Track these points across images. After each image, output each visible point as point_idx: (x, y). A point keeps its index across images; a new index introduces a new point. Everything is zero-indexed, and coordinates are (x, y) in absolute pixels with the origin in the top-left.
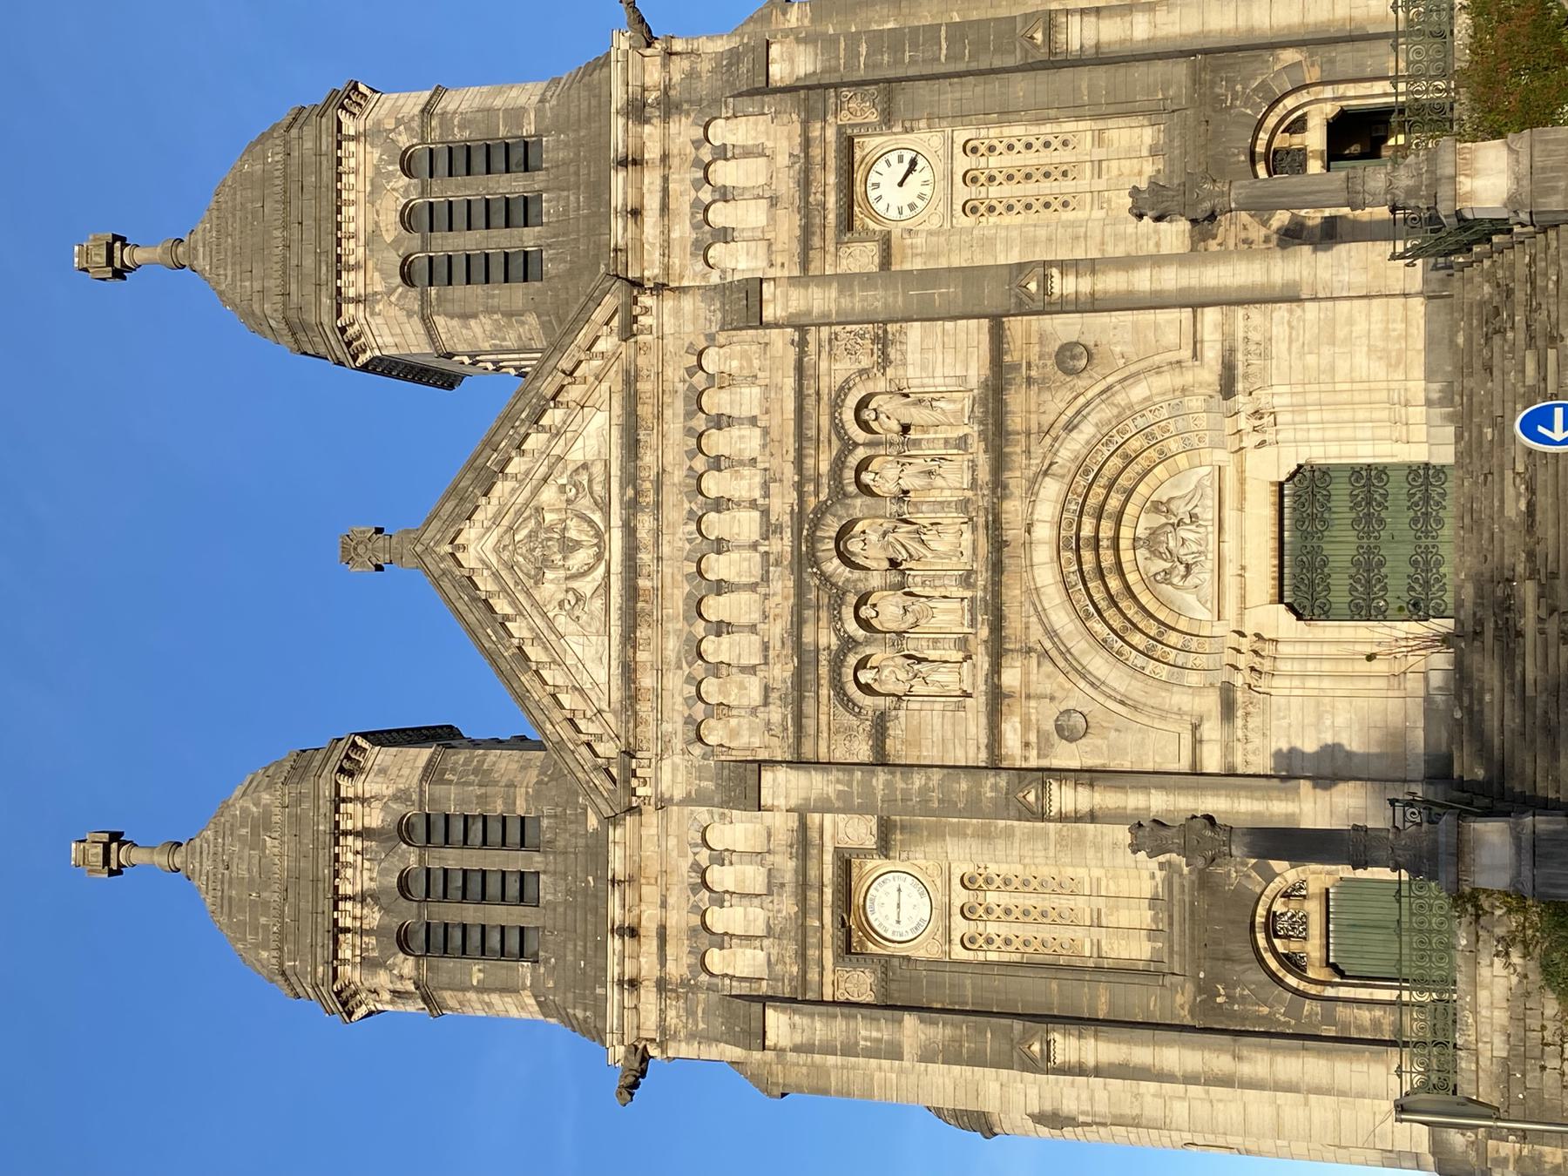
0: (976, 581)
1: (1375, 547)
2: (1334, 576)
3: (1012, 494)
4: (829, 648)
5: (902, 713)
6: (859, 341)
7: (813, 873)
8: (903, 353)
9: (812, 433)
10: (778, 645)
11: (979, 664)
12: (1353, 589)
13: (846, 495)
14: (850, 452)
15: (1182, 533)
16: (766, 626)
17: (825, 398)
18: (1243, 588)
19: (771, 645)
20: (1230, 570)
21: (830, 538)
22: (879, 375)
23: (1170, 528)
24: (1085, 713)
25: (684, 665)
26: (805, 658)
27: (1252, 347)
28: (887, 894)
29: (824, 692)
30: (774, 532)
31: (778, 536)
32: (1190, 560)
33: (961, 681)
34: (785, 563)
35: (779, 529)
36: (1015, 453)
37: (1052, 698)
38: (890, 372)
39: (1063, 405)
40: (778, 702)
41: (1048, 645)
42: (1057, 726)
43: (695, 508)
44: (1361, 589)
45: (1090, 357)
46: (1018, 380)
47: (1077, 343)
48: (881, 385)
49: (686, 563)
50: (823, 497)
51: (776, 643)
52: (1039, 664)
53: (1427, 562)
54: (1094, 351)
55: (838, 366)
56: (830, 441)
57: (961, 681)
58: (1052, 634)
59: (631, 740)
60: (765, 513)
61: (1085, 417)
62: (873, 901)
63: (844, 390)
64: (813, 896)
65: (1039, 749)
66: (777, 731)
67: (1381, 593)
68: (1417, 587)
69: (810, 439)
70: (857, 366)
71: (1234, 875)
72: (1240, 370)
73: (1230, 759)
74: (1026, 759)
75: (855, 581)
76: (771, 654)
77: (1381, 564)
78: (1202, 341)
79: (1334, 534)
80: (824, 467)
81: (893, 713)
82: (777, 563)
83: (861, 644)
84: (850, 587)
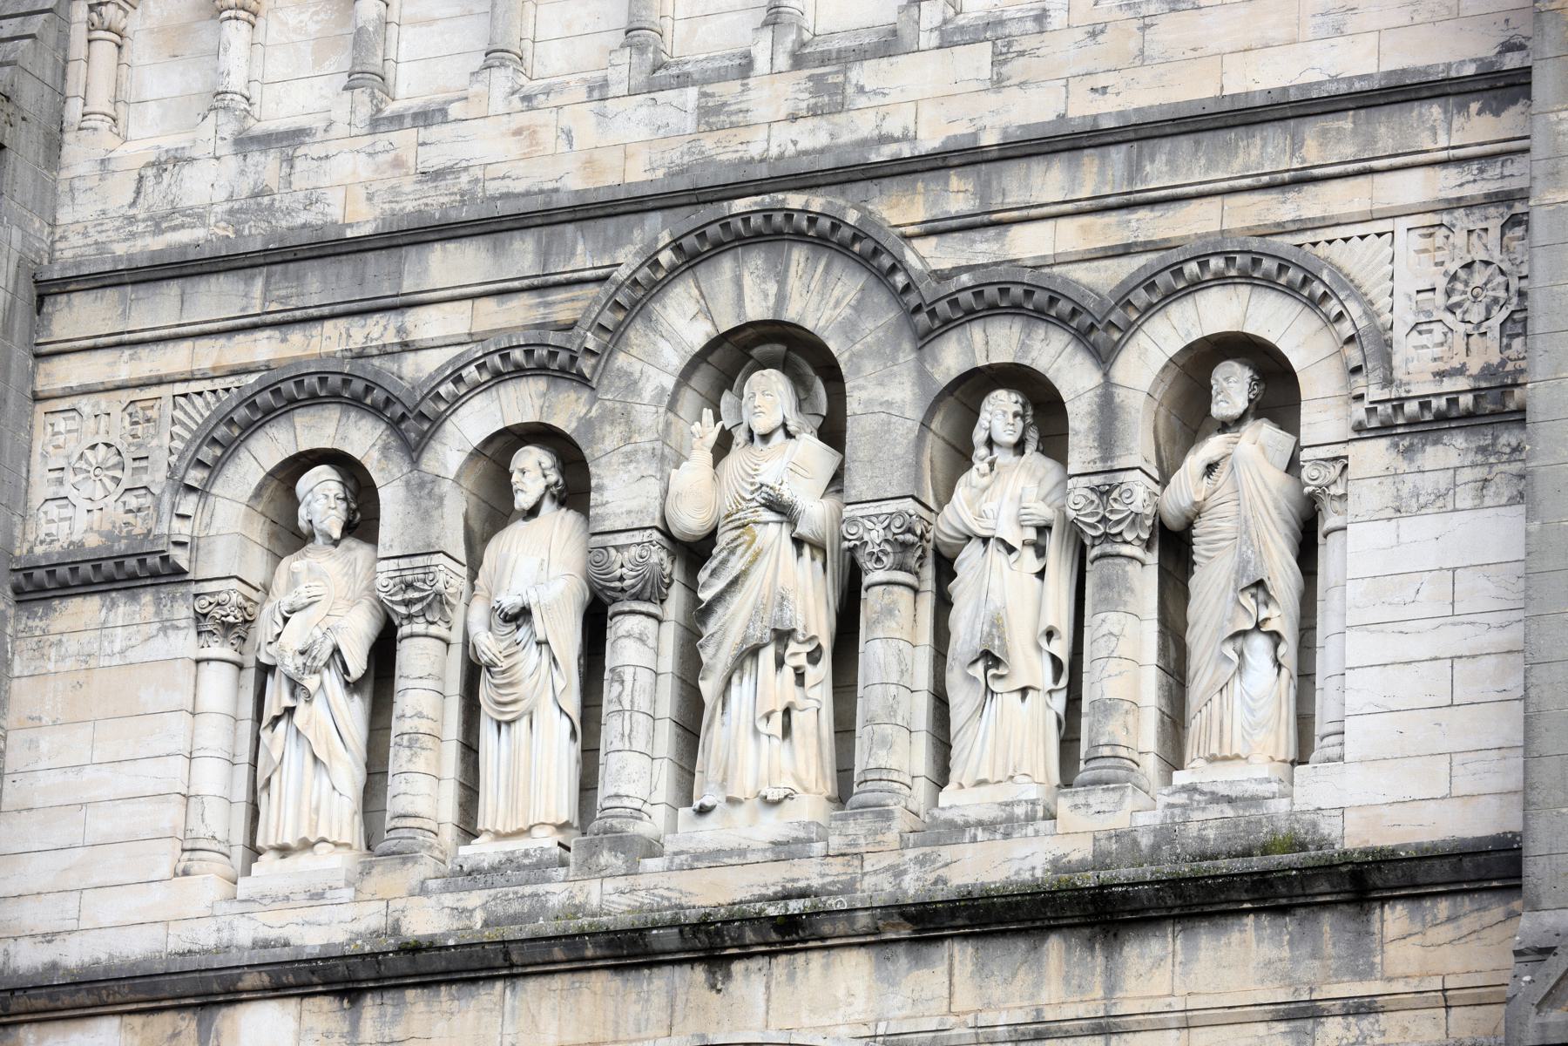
0: (602, 873)
3: (893, 983)
4: (407, 347)
5: (185, 643)
6: (1499, 316)
8: (1442, 500)
9: (1159, 173)
10: (434, 159)
11: (322, 913)
13: (925, 339)
14: (1082, 336)
16: (498, 105)
17: (1282, 208)
19: (434, 132)
21: (781, 298)
26: (374, 262)
29: (263, 348)
33: (284, 851)
34: (709, 144)
36: (1037, 985)
38: (1373, 455)
40: (245, 188)
46: (1309, 970)
51: (442, 147)
55: (1408, 242)
56: (1125, 251)
57: (284, 851)
66: (155, 197)
69: (1134, 170)
70: (1404, 317)
75: (626, 416)
81: (183, 612)
82: (709, 113)
83: (415, 462)
84: (609, 397)
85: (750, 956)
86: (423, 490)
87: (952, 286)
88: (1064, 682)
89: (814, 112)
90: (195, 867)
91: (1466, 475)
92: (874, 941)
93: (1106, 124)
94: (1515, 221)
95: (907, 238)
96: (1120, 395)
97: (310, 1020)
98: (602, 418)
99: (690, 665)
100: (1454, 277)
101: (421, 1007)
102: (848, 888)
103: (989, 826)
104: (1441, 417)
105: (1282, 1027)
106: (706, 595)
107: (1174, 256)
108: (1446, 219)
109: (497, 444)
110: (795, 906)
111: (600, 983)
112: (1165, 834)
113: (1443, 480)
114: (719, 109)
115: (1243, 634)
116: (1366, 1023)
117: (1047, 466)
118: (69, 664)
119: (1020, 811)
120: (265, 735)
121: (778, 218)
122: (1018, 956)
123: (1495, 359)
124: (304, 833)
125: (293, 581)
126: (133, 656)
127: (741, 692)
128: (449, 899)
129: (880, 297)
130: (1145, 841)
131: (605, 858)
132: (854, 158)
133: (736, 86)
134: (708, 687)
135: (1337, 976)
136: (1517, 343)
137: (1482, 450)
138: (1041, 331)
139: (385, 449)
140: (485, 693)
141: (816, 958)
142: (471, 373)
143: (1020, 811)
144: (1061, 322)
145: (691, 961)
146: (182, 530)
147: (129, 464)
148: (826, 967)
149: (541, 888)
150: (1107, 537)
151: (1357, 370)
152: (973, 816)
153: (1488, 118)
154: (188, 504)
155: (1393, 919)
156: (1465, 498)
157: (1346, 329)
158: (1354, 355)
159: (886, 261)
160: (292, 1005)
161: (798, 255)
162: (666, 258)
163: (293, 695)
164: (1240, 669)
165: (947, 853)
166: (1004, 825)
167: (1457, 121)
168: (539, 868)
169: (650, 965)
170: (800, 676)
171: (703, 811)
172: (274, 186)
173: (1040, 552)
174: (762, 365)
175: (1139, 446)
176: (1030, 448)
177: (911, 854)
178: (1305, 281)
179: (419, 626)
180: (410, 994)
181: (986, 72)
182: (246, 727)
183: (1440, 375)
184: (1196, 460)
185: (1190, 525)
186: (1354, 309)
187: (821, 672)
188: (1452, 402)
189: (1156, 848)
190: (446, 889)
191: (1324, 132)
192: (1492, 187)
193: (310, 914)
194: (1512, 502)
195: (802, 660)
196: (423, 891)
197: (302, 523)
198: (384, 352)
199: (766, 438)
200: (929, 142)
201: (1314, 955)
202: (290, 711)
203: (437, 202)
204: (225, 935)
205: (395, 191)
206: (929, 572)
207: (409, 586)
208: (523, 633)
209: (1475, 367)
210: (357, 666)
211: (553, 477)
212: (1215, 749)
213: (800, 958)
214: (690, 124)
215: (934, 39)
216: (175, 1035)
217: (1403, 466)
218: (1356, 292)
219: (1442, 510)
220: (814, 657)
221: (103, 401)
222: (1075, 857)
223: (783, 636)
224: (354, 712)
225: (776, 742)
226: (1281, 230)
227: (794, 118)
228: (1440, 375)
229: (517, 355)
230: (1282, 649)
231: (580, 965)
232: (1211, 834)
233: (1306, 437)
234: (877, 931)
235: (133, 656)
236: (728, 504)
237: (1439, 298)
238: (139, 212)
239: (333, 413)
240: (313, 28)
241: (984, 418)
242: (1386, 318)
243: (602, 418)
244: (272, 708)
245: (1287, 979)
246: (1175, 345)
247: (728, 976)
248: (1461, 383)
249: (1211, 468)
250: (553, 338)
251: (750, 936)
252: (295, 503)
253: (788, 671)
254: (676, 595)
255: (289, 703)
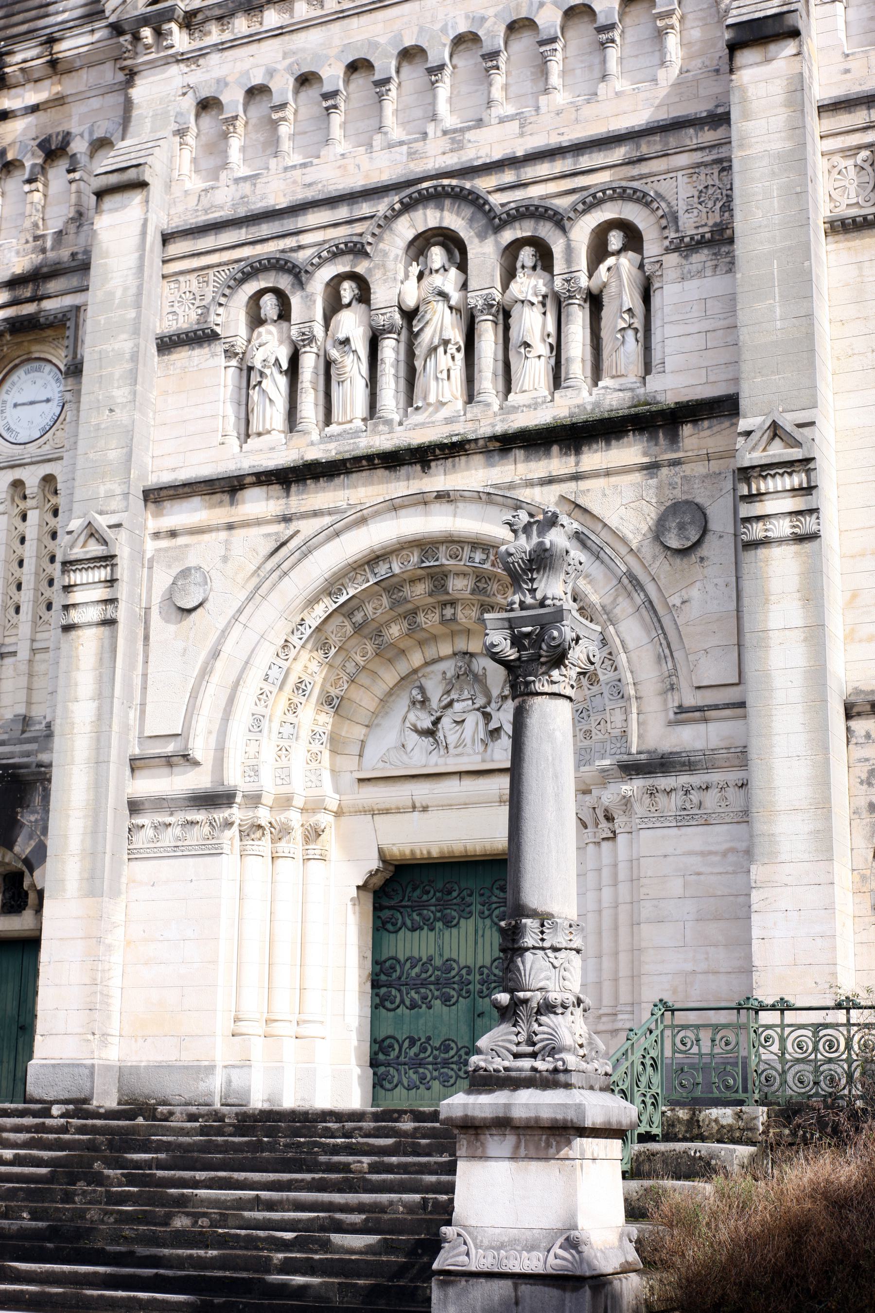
1: (468, 992)
2: (432, 935)
4: (300, 247)
5: (222, 360)
6: (719, 205)
7: (53, 286)
8: (700, 274)
9: (586, 161)
10: (308, 180)
12: (414, 961)
13: (497, 229)
15: (473, 720)
17: (635, 171)
18: (399, 811)
20: (421, 791)
22: (666, 243)
23: (480, 701)
24: (206, 605)
25: (288, 61)
27: (695, 796)
28: (45, 386)
30: (453, 140)
31: (448, 147)
32: (440, 734)
35: (458, 146)
37: (225, 559)
38: (673, 259)
39: (613, 521)
40: (238, 196)
41: (292, 545)
42: (189, 569)
43: (487, 24)
44: (413, 973)
45: (683, 552)
46: (654, 450)
47: (705, 531)
48: (652, 247)
49: (416, 29)
50: (496, 199)
51: (312, 174)
52: (269, 535)
53: (446, 1063)
54: (693, 558)
56: (573, 191)
58: (307, 550)
59: (200, 17)
60: (479, 123)
61: (598, 558)
62: (39, 370)
63: (642, 199)
64: (28, 293)
65: (166, 550)
66: (205, 201)
67: (408, 1003)
68: (415, 1049)
70: (682, 207)
71: (33, 818)
72: (664, 782)
73: (147, 806)
74: (156, 535)
75: (384, 266)
76: (298, 173)
77: (446, 1000)
78: (706, 720)
79: (488, 933)
80: (535, 192)
84: (377, 259)
85: (438, 459)
86: (309, 299)
87: (507, 208)
88: (554, 353)
89: (452, 151)
90: (226, 441)
91: (709, 264)
92: (486, 452)
93: (564, 144)
94: (723, 170)
95: (489, 193)
96: (573, 244)
97: (271, 493)
98: (374, 268)
99: (411, 354)
100: (701, 192)
101: (313, 486)
102: (475, 431)
103: (529, 406)
104: (699, 243)
105: (645, 472)
106: (416, 330)
107: (592, 191)
108: (697, 170)
109: (335, 281)
110: (455, 439)
111: (380, 472)
112: (597, 404)
113: (700, 266)
114: (415, 153)
115: (624, 329)
116: (677, 468)
117: (546, 275)
118: (178, 371)
119: (540, 400)
120: (251, 392)
121: (440, 189)
122: (541, 453)
123: (718, 220)
124: (268, 427)
125: (260, 335)
126: (200, 367)
127: (431, 364)
128: (322, 447)
129: (480, 215)
130: (589, 408)
131: (381, 427)
132: (468, 165)
133: (422, 143)
134: (418, 364)
135: (665, 452)
136: (727, 214)
137: (715, 254)
138: (542, 223)
139: (293, 285)
140: (333, 371)
141: (463, 458)
142: (325, 254)
143: (540, 400)
144: (550, 219)
145: (415, 463)
146: (219, 320)
147: (198, 298)
148: (467, 462)
149: (357, 440)
150: (570, 297)
151: (665, 228)
152: (521, 404)
153: (712, 132)
154: (220, 310)
155: (687, 430)
156: (709, 272)
157: (660, 213)
158: (664, 222)
159: (481, 201)
160: (265, 488)
161: (447, 202)
162: (397, 206)
163: (261, 376)
164: (623, 343)
165: (512, 417)
166: (534, 406)
167: (700, 134)
168: (356, 434)
169: (399, 465)
170: (453, 358)
171: (417, 408)
172: (249, 193)
173: (544, 305)
174: (434, 245)
175: (582, 262)
176: (538, 268)
177: (498, 418)
178: (644, 197)
179: (307, 349)
180: (309, 482)
181: (517, 131)
182: (244, 391)
183: (697, 227)
184: (603, 267)
185: (601, 291)
186: (663, 205)
187: (460, 356)
188: (703, 237)
189: (593, 409)
190: (321, 443)
191: (649, 142)
192: (715, 157)
193: (270, 455)
194: (727, 272)
195: (454, 351)
196: (312, 444)
197: (262, 316)
198: (292, 250)
199: (437, 271)
200: (497, 156)
201: (656, 445)
202: (260, 383)
203: (310, 194)
204: (239, 466)
205: (294, 192)
206: (501, 317)
207: (304, 334)
208: (347, 348)
209: (711, 223)
210: (285, 366)
211: (356, 291)
212: (614, 373)
213: (457, 459)
214: (404, 158)
215: (497, 121)
216: (221, 502)
217: (684, 262)
218: (663, 198)
219: (700, 278)
220: (458, 350)
221: (188, 277)
222: (562, 415)
223: (446, 343)
224: (283, 381)
225: (446, 382)
226: (633, 179)
227: (444, 153)
228: (697, 227)
229: (342, 246)
230: (639, 335)
231: (372, 467)
232: (614, 403)
233: (646, 254)
234: (486, 446)
235: (200, 367)
236: (423, 296)
237: (696, 200)
238: (199, 208)
239: (273, 274)
240: (262, 139)
241: (521, 257)
242: (675, 208)
243: (374, 268)
244: (253, 382)
245: (645, 454)
246: (594, 224)
247: (429, 467)
248: (706, 229)
249: (609, 269)
250: (355, 239)
251: (438, 452)
252: (259, 308)
253: (449, 356)
254: (404, 332)
255: (259, 379)
